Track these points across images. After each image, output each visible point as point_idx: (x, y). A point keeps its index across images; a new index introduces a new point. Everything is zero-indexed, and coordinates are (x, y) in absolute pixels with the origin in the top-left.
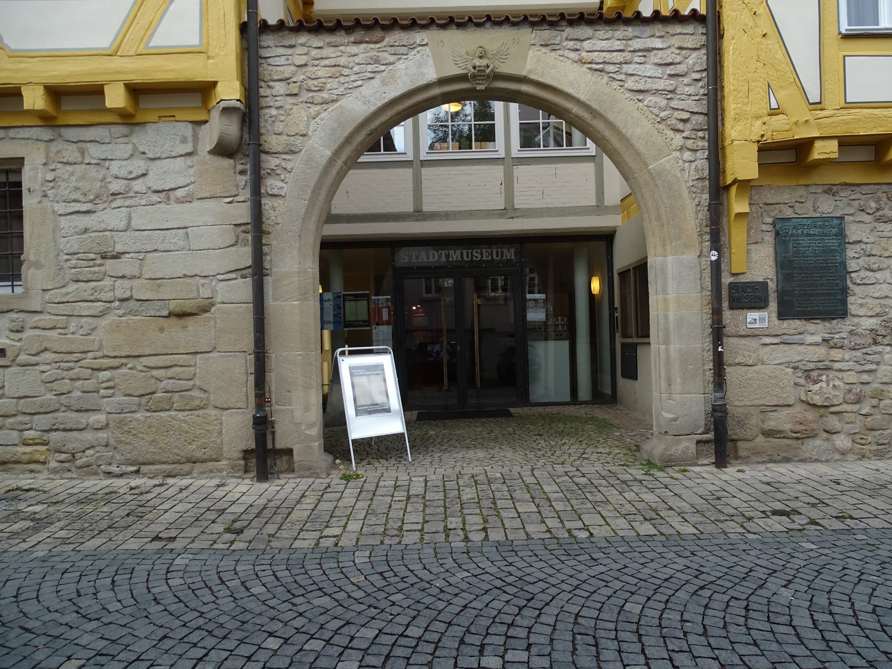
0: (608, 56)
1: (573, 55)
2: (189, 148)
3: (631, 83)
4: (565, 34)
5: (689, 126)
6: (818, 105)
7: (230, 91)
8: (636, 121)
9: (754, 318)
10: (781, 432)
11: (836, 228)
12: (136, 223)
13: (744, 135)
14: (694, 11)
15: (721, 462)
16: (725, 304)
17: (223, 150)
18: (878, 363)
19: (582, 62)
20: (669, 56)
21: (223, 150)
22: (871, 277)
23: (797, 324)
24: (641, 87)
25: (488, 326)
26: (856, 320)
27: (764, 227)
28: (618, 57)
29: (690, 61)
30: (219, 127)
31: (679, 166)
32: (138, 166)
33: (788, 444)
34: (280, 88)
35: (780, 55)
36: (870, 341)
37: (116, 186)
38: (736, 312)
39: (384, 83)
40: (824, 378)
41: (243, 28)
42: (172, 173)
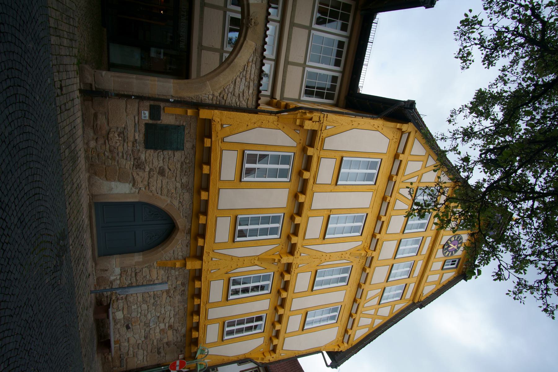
0: (249, 73)
1: (251, 59)
3: (238, 79)
4: (258, 58)
5: (221, 99)
6: (223, 141)
8: (225, 79)
9: (146, 114)
10: (97, 119)
11: (180, 148)
13: (216, 115)
14: (259, 105)
15: (81, 91)
16: (152, 103)
18: (126, 159)
19: (248, 62)
20: (246, 95)
24: (237, 83)
26: (144, 152)
27: (182, 122)
28: (248, 77)
29: (243, 102)
33: (91, 122)
35: (241, 130)
36: (136, 157)
38: (149, 107)
40: (120, 139)
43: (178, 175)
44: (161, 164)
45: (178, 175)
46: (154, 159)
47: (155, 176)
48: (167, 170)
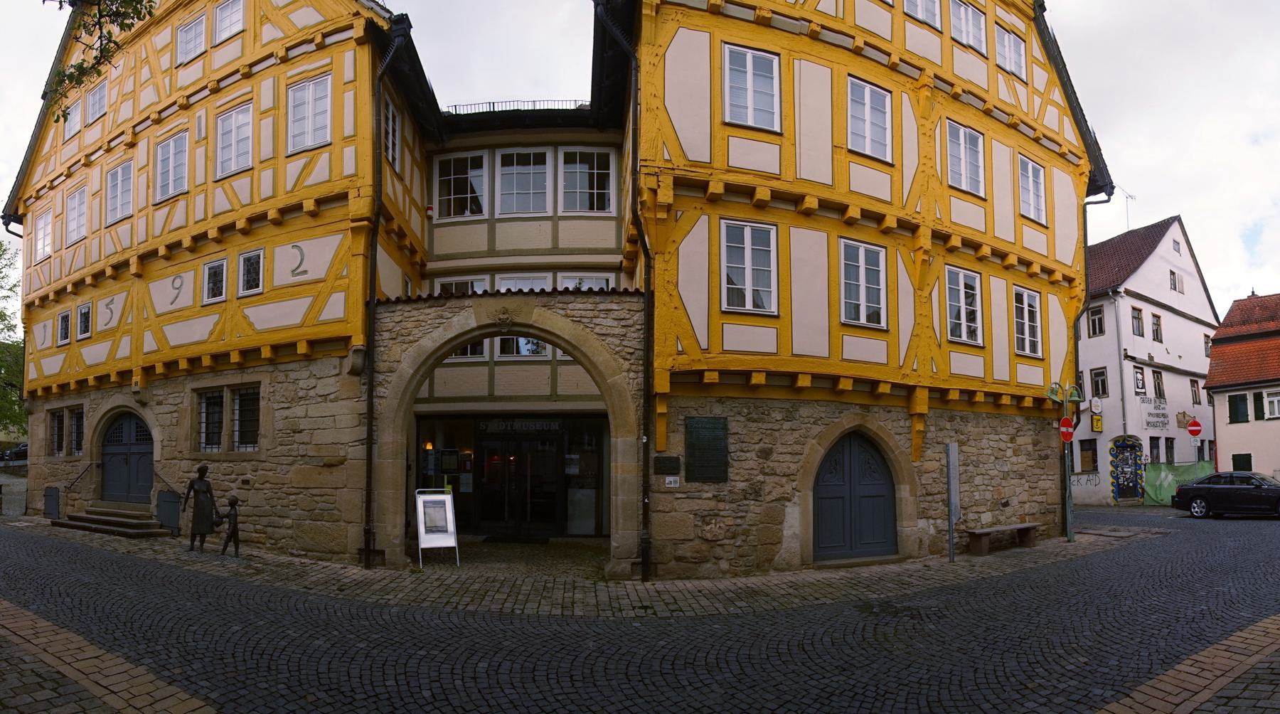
1: (562, 312)
2: (337, 371)
3: (597, 330)
7: (358, 341)
8: (600, 353)
11: (722, 424)
12: (310, 414)
16: (651, 471)
17: (354, 372)
19: (567, 316)
21: (354, 372)
22: (744, 456)
23: (697, 485)
25: (525, 475)
28: (590, 314)
30: (351, 361)
31: (626, 380)
32: (312, 382)
34: (386, 335)
37: (301, 394)
39: (445, 330)
41: (367, 304)
42: (329, 386)
43: (770, 426)
44: (753, 455)
45: (770, 426)
46: (743, 467)
47: (771, 464)
48: (762, 444)
